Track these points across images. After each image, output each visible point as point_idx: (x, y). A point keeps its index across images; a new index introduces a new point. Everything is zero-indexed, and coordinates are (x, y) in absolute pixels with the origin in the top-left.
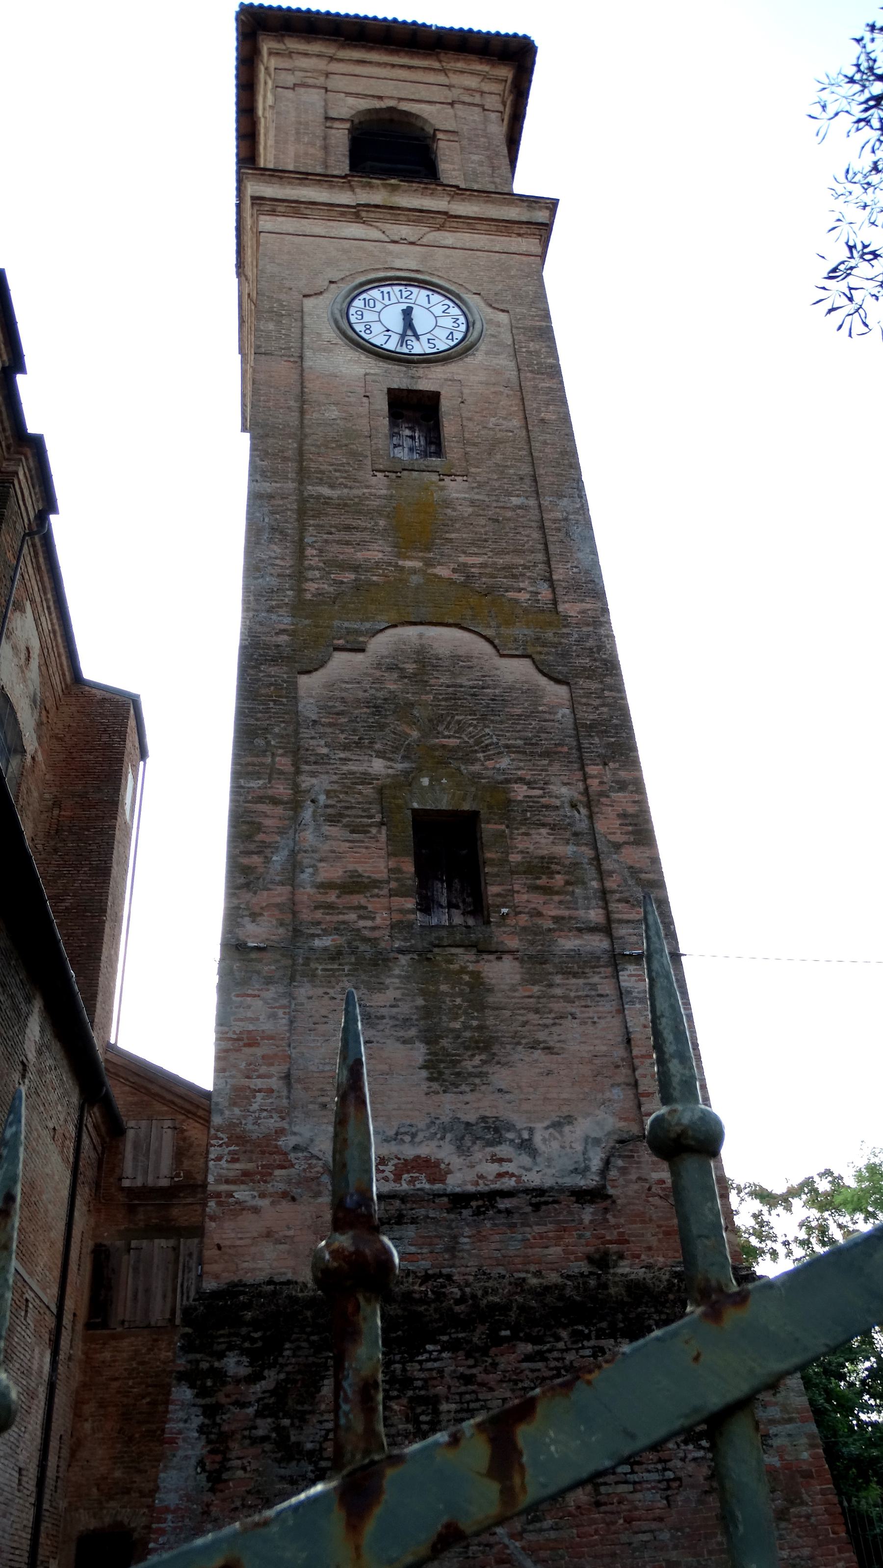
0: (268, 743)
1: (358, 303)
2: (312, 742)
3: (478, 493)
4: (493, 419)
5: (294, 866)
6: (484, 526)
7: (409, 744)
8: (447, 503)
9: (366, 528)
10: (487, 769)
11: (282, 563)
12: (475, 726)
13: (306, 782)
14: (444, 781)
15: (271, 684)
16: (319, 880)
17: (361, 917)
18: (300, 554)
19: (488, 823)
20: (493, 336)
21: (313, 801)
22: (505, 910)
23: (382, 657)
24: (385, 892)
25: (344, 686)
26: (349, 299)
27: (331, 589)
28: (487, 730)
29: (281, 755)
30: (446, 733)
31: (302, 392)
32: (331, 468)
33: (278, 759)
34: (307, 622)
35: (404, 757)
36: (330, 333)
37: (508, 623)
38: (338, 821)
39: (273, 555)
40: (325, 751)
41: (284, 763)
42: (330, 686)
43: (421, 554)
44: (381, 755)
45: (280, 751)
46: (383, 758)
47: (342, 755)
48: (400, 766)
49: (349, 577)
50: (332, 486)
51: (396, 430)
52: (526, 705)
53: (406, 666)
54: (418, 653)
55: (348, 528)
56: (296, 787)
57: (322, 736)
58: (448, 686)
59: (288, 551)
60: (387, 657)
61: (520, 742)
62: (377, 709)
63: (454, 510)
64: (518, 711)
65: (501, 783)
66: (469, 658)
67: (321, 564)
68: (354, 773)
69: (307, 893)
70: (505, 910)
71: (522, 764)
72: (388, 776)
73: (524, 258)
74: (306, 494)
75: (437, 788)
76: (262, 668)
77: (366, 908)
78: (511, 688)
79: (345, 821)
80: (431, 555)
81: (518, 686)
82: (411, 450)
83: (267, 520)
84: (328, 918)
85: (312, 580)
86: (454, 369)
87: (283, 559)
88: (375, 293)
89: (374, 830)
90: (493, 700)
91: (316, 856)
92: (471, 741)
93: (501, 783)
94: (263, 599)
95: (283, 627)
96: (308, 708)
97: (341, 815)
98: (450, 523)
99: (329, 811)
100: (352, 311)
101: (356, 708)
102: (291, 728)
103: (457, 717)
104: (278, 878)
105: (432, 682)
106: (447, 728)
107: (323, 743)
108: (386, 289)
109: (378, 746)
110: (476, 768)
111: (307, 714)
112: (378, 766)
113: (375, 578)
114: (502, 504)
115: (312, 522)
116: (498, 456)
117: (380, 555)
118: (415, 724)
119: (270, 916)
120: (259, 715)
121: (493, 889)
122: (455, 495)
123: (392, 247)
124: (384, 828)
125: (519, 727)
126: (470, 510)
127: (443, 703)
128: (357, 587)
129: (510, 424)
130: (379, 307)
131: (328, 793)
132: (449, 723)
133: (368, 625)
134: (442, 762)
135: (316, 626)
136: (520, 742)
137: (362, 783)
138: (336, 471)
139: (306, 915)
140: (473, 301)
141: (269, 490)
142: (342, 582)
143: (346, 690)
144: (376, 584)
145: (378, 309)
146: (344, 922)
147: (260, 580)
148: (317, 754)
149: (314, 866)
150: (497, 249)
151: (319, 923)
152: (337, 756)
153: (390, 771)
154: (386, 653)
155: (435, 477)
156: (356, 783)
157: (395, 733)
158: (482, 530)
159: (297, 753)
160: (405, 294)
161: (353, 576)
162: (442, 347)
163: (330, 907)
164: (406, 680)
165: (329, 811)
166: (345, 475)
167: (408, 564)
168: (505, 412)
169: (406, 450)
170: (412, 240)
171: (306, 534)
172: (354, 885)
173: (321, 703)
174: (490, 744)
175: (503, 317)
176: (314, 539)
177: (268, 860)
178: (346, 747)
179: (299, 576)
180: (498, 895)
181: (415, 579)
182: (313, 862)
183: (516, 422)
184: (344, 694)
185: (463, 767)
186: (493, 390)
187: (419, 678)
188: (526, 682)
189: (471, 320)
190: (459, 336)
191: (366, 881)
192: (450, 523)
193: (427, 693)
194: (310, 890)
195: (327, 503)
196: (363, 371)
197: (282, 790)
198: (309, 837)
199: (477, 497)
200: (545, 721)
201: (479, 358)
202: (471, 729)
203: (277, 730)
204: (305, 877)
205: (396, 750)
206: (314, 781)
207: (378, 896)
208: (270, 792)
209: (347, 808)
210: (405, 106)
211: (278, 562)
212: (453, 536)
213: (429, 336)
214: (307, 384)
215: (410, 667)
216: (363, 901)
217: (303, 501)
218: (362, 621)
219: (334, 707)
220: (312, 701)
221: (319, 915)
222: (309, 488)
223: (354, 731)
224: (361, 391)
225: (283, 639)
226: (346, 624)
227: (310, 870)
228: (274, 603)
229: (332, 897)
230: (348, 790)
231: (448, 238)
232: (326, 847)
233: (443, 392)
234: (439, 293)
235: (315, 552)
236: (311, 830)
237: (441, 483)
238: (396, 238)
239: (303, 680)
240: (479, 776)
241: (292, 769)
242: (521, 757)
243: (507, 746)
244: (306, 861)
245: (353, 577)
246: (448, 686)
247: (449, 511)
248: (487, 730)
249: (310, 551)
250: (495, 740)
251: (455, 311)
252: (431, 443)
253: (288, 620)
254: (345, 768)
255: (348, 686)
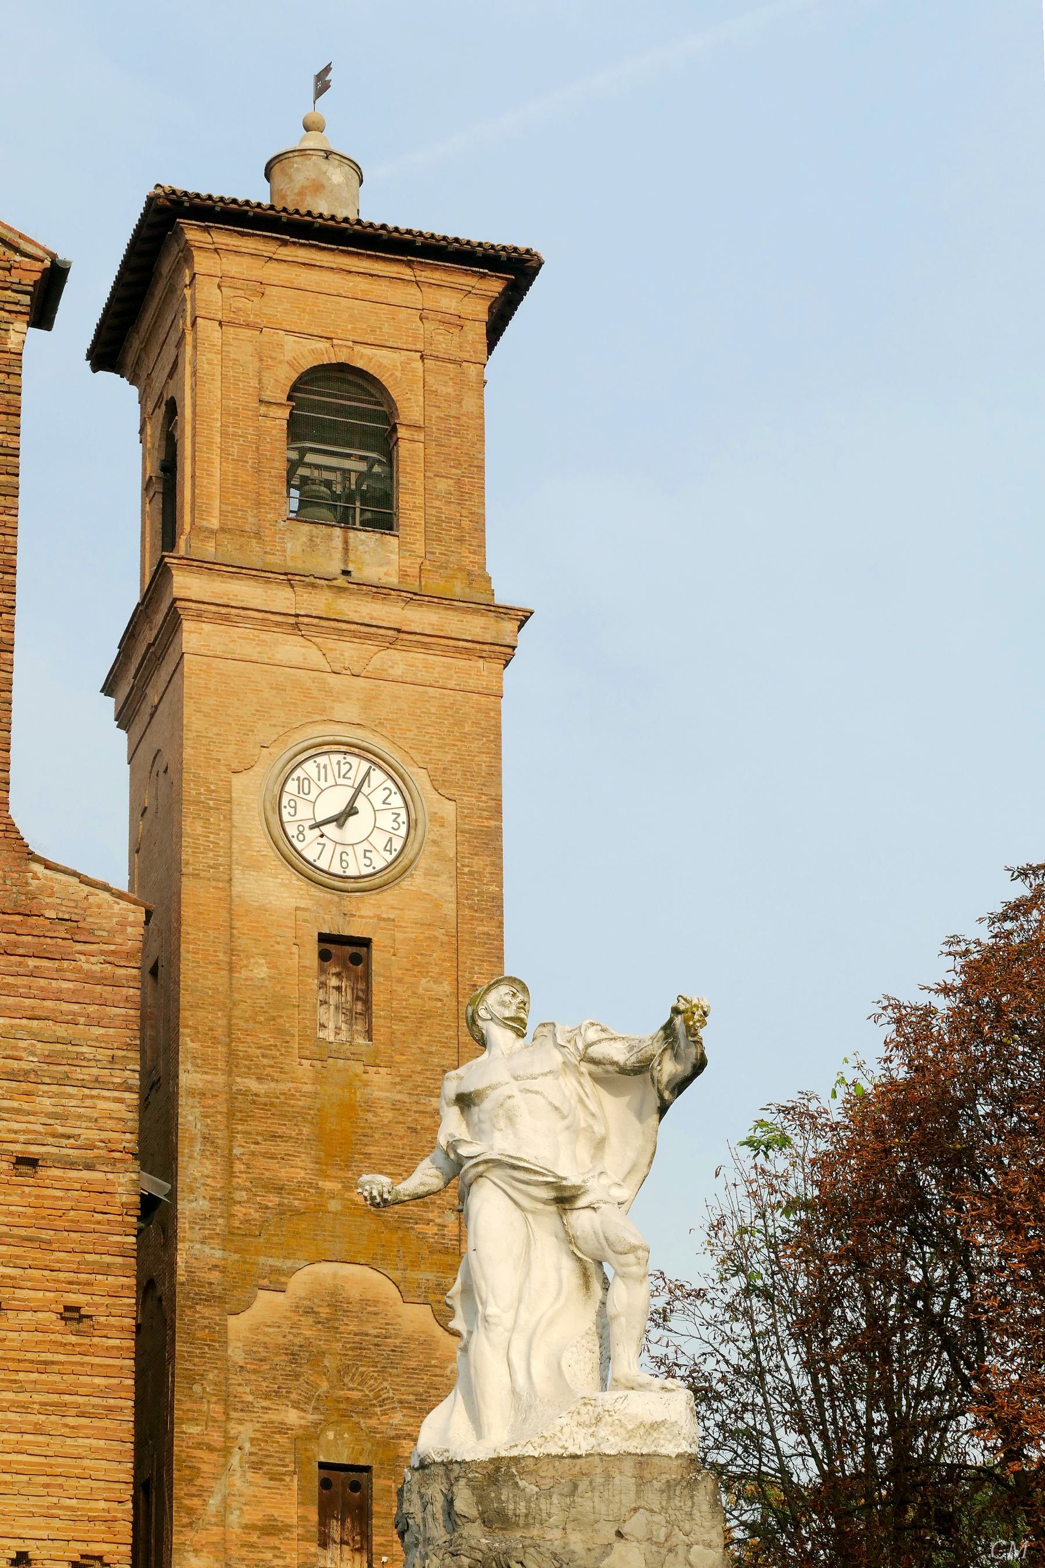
0: (204, 1389)
1: (291, 786)
2: (240, 1389)
3: (400, 1092)
4: (424, 981)
5: (225, 1508)
6: (402, 1138)
7: (319, 1396)
8: (369, 1106)
9: (291, 1137)
10: (381, 1423)
11: (213, 1184)
12: (376, 1379)
13: (234, 1428)
14: (346, 1435)
15: (206, 1327)
16: (244, 1522)
17: (275, 1556)
18: (230, 1174)
19: (379, 1477)
20: (434, 842)
21: (240, 1448)
22: (384, 1559)
23: (300, 1299)
24: (295, 1535)
25: (266, 1329)
26: (281, 779)
27: (256, 1215)
28: (385, 1384)
29: (215, 1403)
30: (351, 1385)
31: (232, 935)
32: (258, 1052)
33: (212, 1406)
34: (236, 1257)
35: (315, 1408)
36: (260, 841)
37: (414, 1265)
38: (260, 1469)
39: (206, 1172)
40: (250, 1398)
41: (217, 1409)
42: (255, 1329)
43: (340, 1173)
44: (296, 1405)
45: (214, 1399)
46: (297, 1408)
47: (265, 1403)
48: (312, 1417)
49: (273, 1200)
50: (259, 1079)
51: (323, 979)
52: (421, 1358)
53: (321, 1310)
54: (332, 1294)
55: (274, 1137)
56: (227, 1436)
57: (248, 1382)
58: (356, 1334)
59: (219, 1168)
60: (305, 1299)
61: (412, 1398)
62: (294, 1357)
63: (376, 1115)
64: (413, 1364)
65: (393, 1438)
66: (376, 1303)
67: (248, 1184)
68: (272, 1423)
69: (235, 1530)
70: (384, 1559)
71: (411, 1420)
72: (301, 1426)
73: (483, 700)
74: (234, 1088)
75: (339, 1442)
76: (198, 1308)
77: (279, 1549)
78: (409, 1339)
79: (265, 1468)
80: (350, 1174)
81: (416, 1336)
82: (337, 1008)
83: (199, 1126)
84: (251, 1555)
85: (240, 1202)
86: (389, 897)
87: (213, 1178)
88: (310, 767)
89: (287, 1478)
90: (393, 1351)
91: (243, 1500)
92: (371, 1394)
93: (393, 1438)
94: (197, 1227)
95: (215, 1262)
96: (236, 1353)
97: (262, 1463)
98: (370, 1131)
99: (253, 1458)
100: (284, 802)
101: (276, 1355)
102: (222, 1376)
103: (361, 1369)
104: (213, 1520)
105: (342, 1329)
106: (352, 1380)
107: (248, 1390)
108: (322, 760)
109: (294, 1396)
110: (373, 1422)
111: (235, 1358)
112: (292, 1417)
113: (296, 1203)
114: (421, 1108)
115: (240, 1127)
116: (424, 1038)
117: (302, 1173)
118: (325, 1374)
119: (209, 1552)
120: (196, 1360)
121: (377, 1540)
122: (377, 1094)
123: (332, 679)
124: (296, 1477)
125: (413, 1382)
126: (390, 1114)
127: (350, 1353)
128: (282, 1211)
129: (440, 989)
130: (315, 791)
131: (252, 1440)
132: (354, 1375)
133: (289, 1263)
134: (345, 1415)
135: (245, 1262)
136: (412, 1398)
137: (280, 1433)
138: (263, 1056)
139: (235, 1552)
140: (420, 779)
141: (200, 1085)
142: (267, 1208)
143: (266, 1334)
144: (298, 1213)
145: (312, 797)
146: (263, 1560)
147: (194, 1204)
148: (242, 1402)
149: (240, 1509)
150: (452, 684)
151: (244, 1559)
152: (259, 1405)
153: (303, 1422)
154: (303, 1295)
155: (359, 1068)
156: (275, 1433)
157: (307, 1383)
158: (400, 1143)
159: (227, 1400)
160: (344, 768)
161: (277, 1200)
162: (379, 864)
163: (252, 1545)
164: (319, 1326)
165: (253, 1458)
166: (272, 1063)
167: (328, 1185)
168: (437, 970)
169: (332, 1008)
170: (356, 671)
171: (235, 1143)
172: (271, 1528)
173: (247, 1348)
174: (388, 1398)
175: (450, 806)
176: (242, 1150)
177: (205, 1503)
178: (267, 1396)
179: (229, 1201)
180: (381, 1545)
181: (334, 1205)
182: (240, 1505)
183: (446, 987)
184: (267, 1339)
185: (362, 1421)
186: (427, 933)
187: (331, 1324)
188: (423, 1332)
189: (413, 816)
190: (398, 844)
191: (280, 1524)
192: (370, 1131)
193: (337, 1341)
194: (239, 1531)
195: (254, 1102)
196: (293, 903)
197: (215, 1438)
198: (238, 1481)
199: (399, 1097)
200: (435, 1376)
201: (416, 882)
202: (372, 1382)
203: (211, 1376)
204: (233, 1518)
205: (309, 1399)
206: (241, 1428)
207: (288, 1539)
208: (206, 1439)
209: (267, 1456)
210: (364, 359)
211: (209, 1181)
212: (371, 1150)
213: (366, 846)
214: (237, 924)
215: (324, 1312)
216: (277, 1543)
217: (232, 1098)
218: (285, 1257)
219: (258, 1352)
220: (240, 1345)
221: (244, 1552)
222: (238, 1079)
223: (274, 1379)
224: (290, 933)
225: (215, 1276)
226: (271, 1261)
227: (237, 1512)
228: (207, 1232)
229: (254, 1538)
230: (267, 1439)
231: (398, 662)
232: (249, 1491)
233: (374, 939)
234: (380, 768)
235: (243, 1167)
236: (238, 1474)
237: (365, 1076)
238: (337, 667)
239: (232, 1320)
240: (373, 1430)
241: (224, 1418)
242: (412, 1413)
243: (401, 1402)
244: (235, 1505)
245: (277, 1200)
246: (356, 1334)
247: (370, 1116)
248: (385, 1384)
249: (239, 1166)
250: (391, 1395)
251: (397, 800)
252: (358, 998)
253: (218, 1254)
254: (266, 1416)
255: (270, 1330)
